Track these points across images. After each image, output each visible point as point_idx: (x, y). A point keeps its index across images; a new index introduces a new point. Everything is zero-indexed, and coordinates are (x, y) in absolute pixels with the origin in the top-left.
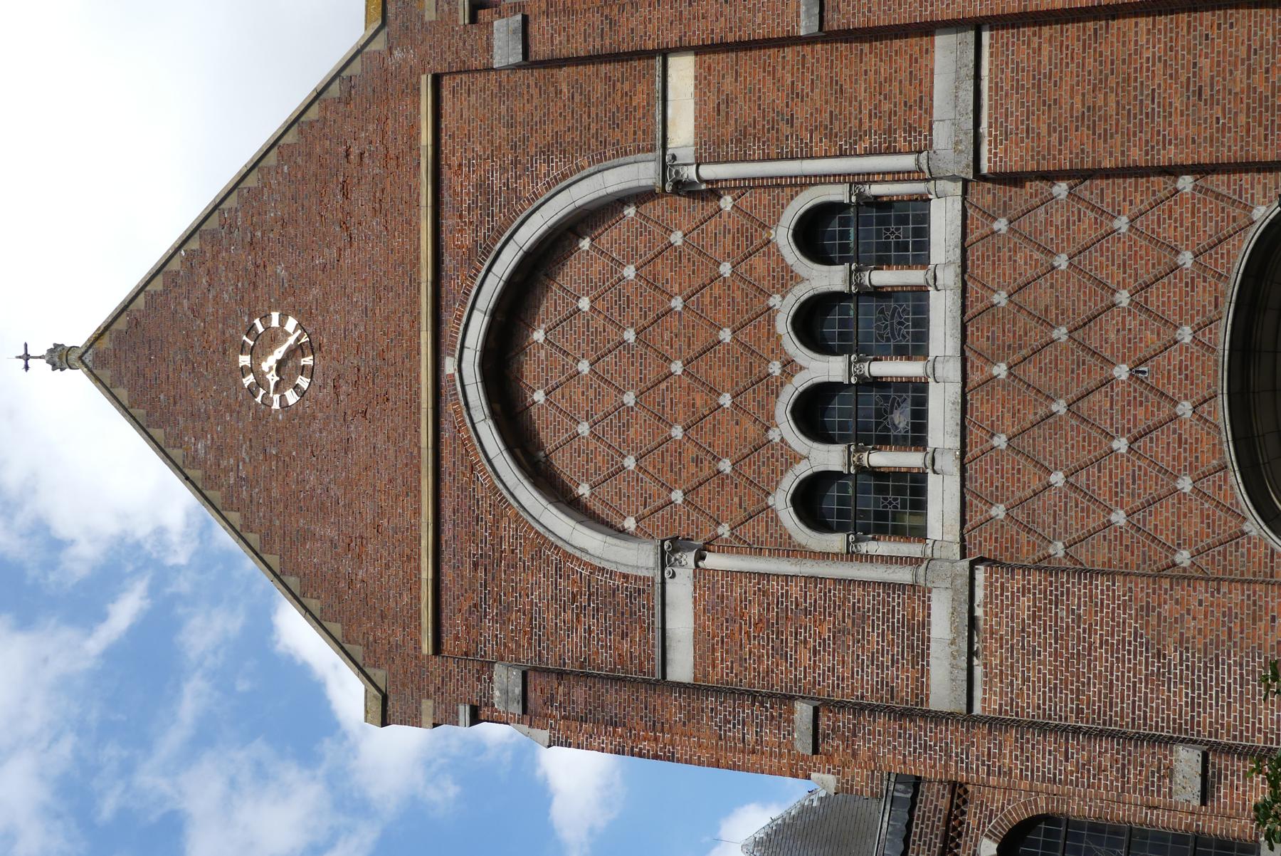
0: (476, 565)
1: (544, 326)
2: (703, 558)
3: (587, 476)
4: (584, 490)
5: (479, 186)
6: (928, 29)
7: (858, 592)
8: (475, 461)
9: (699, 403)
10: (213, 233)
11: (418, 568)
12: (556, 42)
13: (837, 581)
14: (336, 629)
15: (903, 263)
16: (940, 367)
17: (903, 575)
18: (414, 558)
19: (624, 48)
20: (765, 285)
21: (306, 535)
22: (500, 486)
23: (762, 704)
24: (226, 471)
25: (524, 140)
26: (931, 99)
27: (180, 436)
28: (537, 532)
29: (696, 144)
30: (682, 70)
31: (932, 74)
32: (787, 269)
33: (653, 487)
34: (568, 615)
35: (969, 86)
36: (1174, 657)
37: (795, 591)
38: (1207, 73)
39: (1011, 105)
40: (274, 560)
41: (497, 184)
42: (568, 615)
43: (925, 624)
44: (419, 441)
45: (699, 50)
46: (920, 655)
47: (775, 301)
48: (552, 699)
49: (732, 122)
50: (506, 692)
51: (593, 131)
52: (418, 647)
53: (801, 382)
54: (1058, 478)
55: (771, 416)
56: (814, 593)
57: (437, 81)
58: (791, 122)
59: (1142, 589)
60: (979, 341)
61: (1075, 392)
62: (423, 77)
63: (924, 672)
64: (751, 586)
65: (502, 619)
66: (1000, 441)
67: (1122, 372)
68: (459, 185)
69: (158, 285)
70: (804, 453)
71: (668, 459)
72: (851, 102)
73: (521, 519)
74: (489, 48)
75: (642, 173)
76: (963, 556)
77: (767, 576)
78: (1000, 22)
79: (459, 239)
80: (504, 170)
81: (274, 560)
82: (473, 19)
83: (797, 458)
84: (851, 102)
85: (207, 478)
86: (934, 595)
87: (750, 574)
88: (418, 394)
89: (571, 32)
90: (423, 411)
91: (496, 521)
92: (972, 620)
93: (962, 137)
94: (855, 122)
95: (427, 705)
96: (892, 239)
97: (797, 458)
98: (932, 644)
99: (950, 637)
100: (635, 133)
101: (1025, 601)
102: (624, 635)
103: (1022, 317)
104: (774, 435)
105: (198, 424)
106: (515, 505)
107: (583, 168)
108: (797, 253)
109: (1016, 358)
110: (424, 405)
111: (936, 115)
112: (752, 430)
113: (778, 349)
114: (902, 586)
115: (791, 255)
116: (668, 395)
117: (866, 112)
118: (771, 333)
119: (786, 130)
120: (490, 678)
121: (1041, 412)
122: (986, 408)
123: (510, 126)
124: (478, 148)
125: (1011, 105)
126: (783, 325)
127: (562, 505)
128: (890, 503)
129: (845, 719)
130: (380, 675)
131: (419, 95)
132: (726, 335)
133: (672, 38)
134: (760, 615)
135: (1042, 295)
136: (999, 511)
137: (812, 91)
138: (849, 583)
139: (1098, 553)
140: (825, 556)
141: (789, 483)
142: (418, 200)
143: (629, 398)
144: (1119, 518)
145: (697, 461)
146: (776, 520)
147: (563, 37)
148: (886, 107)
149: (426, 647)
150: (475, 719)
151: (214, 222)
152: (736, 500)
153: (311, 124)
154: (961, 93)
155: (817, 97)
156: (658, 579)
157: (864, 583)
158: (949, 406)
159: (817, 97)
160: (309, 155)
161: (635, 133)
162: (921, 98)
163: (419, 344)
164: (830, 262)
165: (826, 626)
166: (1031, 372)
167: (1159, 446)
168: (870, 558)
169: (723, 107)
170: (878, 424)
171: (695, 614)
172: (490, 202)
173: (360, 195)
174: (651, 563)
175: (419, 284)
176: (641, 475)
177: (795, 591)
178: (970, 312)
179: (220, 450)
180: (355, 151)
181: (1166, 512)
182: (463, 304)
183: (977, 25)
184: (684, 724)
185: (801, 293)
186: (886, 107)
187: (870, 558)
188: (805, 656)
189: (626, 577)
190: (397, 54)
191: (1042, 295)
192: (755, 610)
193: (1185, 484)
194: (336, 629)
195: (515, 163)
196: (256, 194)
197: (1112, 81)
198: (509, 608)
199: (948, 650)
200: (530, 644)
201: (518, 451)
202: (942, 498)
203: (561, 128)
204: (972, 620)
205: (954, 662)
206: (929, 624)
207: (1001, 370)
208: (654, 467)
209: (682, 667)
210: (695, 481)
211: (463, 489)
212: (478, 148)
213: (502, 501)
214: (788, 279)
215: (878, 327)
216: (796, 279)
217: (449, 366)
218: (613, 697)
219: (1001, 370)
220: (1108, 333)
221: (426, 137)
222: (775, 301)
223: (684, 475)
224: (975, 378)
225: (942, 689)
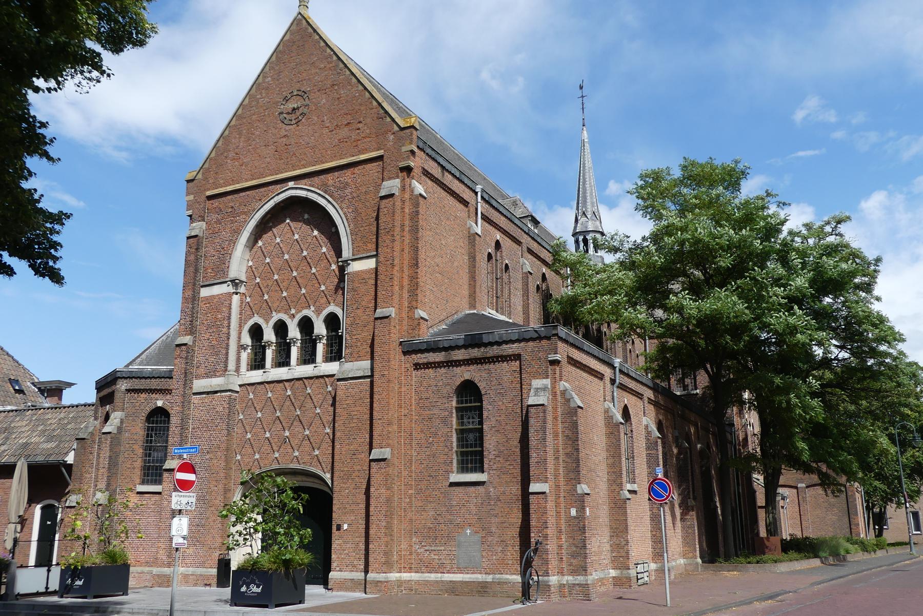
4: (260, 243)
5: (347, 184)
6: (372, 358)
7: (224, 352)
8: (262, 201)
10: (337, 66)
13: (228, 345)
14: (213, 155)
16: (299, 371)
17: (232, 365)
18: (234, 182)
19: (380, 239)
20: (317, 304)
21: (240, 134)
24: (261, 93)
27: (273, 68)
30: (371, 264)
35: (362, 374)
36: (207, 457)
38: (359, 456)
39: (356, 390)
40: (233, 123)
43: (216, 376)
45: (376, 269)
46: (208, 375)
47: (312, 308)
52: (209, 189)
54: (259, 415)
55: (279, 312)
56: (224, 337)
57: (380, 158)
59: (224, 446)
60: (298, 383)
61: (281, 418)
65: (218, 222)
66: (270, 395)
67: (287, 433)
69: (322, 44)
73: (246, 222)
74: (390, 179)
75: (346, 253)
76: (240, 386)
77: (229, 318)
78: (372, 383)
79: (330, 178)
80: (351, 193)
81: (233, 123)
82: (402, 169)
83: (267, 322)
85: (259, 84)
88: (282, 173)
91: (245, 213)
92: (216, 392)
94: (355, 333)
95: (191, 197)
97: (267, 322)
101: (221, 409)
103: (303, 398)
105: (276, 76)
109: (292, 397)
113: (298, 311)
114: (226, 366)
115: (325, 312)
118: (303, 308)
121: (277, 408)
122: (279, 389)
125: (356, 390)
126: (306, 312)
129: (184, 354)
130: (200, 176)
132: (303, 291)
133: (381, 259)
135: (309, 405)
136: (251, 396)
138: (227, 348)
139: (238, 429)
143: (286, 257)
144: (249, 436)
149: (209, 193)
150: (190, 216)
151: (342, 65)
153: (371, 103)
157: (227, 354)
160: (361, 105)
166: (288, 403)
167: (266, 447)
168: (239, 353)
172: (339, 188)
173: (344, 132)
179: (267, 89)
180: (360, 125)
181: (250, 451)
182: (310, 185)
183: (372, 376)
187: (239, 353)
188: (207, 336)
190: (392, 137)
191: (309, 405)
193: (257, 456)
194: (213, 155)
196: (350, 83)
197: (360, 424)
198: (220, 223)
202: (256, 376)
203: (363, 214)
204: (216, 392)
207: (289, 393)
209: (205, 292)
211: (254, 197)
213: (249, 214)
214: (318, 312)
217: (291, 184)
218: (192, 269)
219: (289, 393)
220: (297, 428)
221: (363, 157)
222: (312, 308)
224: (287, 384)
225: (200, 384)
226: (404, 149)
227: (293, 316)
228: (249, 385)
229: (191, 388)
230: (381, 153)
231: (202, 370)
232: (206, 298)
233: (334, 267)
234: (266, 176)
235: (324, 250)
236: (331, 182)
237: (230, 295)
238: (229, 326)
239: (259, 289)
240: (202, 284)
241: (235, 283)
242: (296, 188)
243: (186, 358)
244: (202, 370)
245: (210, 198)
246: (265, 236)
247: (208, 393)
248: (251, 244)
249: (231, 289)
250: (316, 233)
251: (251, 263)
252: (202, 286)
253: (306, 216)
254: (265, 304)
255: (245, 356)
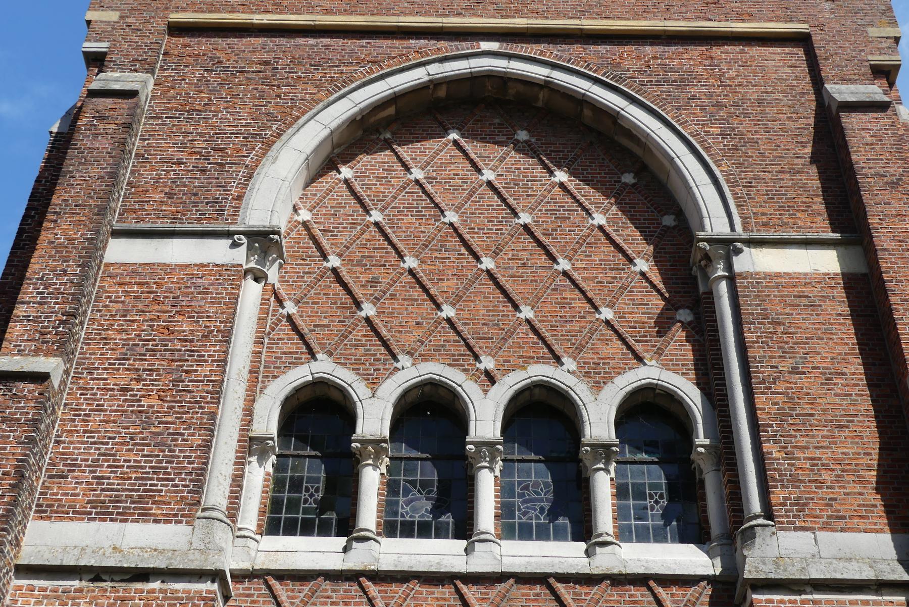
0: (267, 63)
1: (533, 140)
2: (257, 280)
3: (361, 177)
4: (346, 172)
7: (197, 440)
9: (444, 285)
11: (266, 12)
12: (863, 134)
15: (620, 514)
20: (588, 355)
22: (353, 85)
23: (62, 322)
25: (746, 114)
26: (842, 530)
28: (298, 118)
29: (757, 273)
31: (877, 531)
32: (609, 378)
33: (344, 238)
34: (200, 144)
35: (867, 574)
37: (205, 370)
41: (694, 90)
42: (200, 144)
43: (145, 516)
44: (406, 15)
46: (103, 510)
47: (569, 363)
48: (102, 118)
49: (787, 311)
50: (116, 80)
51: (762, 175)
53: (469, 389)
55: (425, 358)
56: (199, 390)
58: (794, 371)
62: (806, 26)
63: (80, 515)
64: (217, 323)
68: (690, 58)
70: (379, 393)
71: (377, 254)
72: (828, 437)
77: (227, 338)
79: (630, 57)
80: (710, 95)
83: (374, 384)
84: (828, 437)
86: (183, 529)
87: (230, 322)
89: (877, 147)
90: (439, 19)
91: (313, 82)
92: (142, 575)
93: (798, 566)
94: (803, 441)
96: (649, 502)
97: (374, 384)
98: (117, 525)
99: (125, 547)
100: (764, 214)
102: (170, 195)
104: (404, 360)
106: (331, 98)
107: (718, 166)
108: (629, 388)
110: (445, 20)
111: (821, 535)
112: (410, 338)
113: (507, 368)
116: (453, 256)
117: (818, 454)
118: (528, 360)
119: (785, 366)
120: (136, 71)
123: (760, 102)
124: (732, 73)
127: (327, 149)
128: (311, 496)
131: (786, 22)
134: (179, 332)
137: (836, 395)
138: (210, 429)
140: (249, 413)
141: (343, 376)
142: (670, 19)
145: (374, 283)
146: (297, 363)
147: (869, 140)
148: (826, 477)
152: (325, 321)
154: (854, 565)
155: (830, 399)
156: (233, 228)
157: (207, 446)
158: (436, 559)
159: (830, 399)
161: (764, 214)
162: (844, 518)
163: (514, 17)
164: (619, 423)
165: (156, 402)
168: (240, 463)
169: (805, 301)
170: (413, 483)
171: (187, 266)
174: (252, 223)
175: (579, 18)
176: (359, 227)
177: (205, 370)
178: (560, 587)
184: (53, 243)
185: (580, 391)
186: (826, 477)
189: (239, 198)
192: (186, 326)
195: (719, 106)
199: (107, 544)
200: (171, 109)
201: (391, 111)
205: (88, 551)
206: (145, 521)
208: (368, 240)
210: (347, 279)
212: (732, 73)
215: (536, 484)
216: (597, 387)
222: (569, 363)
223: (359, 269)
226: (873, 32)
227: (491, 379)
228: (283, 576)
229: (17, 544)
230: (802, 27)
231: (77, 489)
232: (131, 269)
233: (642, 265)
234: (403, 13)
235: (599, 219)
236: (629, 63)
237: (235, 275)
238: (223, 362)
239: (338, 291)
240: (117, 226)
241: (263, 241)
242: (510, 57)
243: (34, 424)
244: (77, 489)
245: (177, 30)
246: (366, 158)
247: (97, 574)
248: (313, 170)
249: (240, 256)
250: (561, 176)
251: (305, 215)
252: (118, 234)
253: (522, 135)
254: (366, 330)
255: (258, 475)
